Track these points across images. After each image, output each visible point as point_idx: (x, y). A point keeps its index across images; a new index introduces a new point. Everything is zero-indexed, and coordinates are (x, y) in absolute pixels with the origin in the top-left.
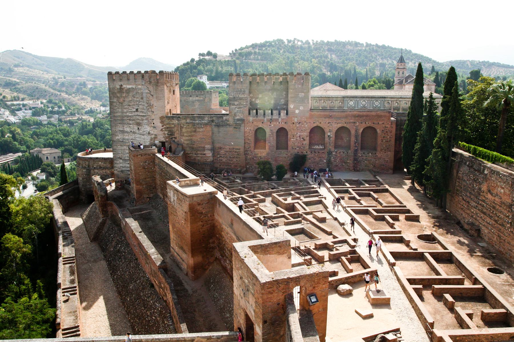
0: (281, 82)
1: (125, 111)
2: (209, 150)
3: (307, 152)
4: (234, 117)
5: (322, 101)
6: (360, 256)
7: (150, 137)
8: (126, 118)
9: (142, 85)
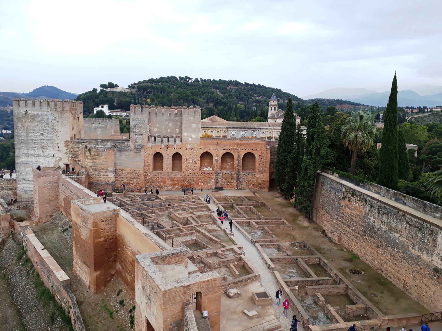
0: (176, 114)
1: (30, 135)
2: (111, 171)
3: (198, 173)
4: (135, 143)
5: (210, 131)
6: (245, 262)
7: (54, 159)
8: (30, 142)
9: (48, 112)
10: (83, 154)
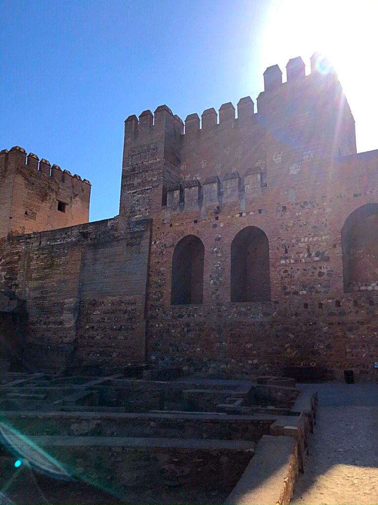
3: (338, 304)
10: (26, 268)
